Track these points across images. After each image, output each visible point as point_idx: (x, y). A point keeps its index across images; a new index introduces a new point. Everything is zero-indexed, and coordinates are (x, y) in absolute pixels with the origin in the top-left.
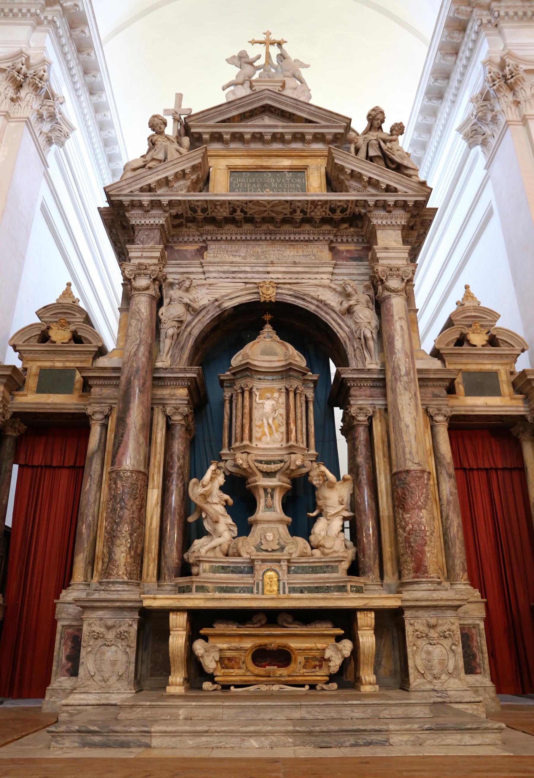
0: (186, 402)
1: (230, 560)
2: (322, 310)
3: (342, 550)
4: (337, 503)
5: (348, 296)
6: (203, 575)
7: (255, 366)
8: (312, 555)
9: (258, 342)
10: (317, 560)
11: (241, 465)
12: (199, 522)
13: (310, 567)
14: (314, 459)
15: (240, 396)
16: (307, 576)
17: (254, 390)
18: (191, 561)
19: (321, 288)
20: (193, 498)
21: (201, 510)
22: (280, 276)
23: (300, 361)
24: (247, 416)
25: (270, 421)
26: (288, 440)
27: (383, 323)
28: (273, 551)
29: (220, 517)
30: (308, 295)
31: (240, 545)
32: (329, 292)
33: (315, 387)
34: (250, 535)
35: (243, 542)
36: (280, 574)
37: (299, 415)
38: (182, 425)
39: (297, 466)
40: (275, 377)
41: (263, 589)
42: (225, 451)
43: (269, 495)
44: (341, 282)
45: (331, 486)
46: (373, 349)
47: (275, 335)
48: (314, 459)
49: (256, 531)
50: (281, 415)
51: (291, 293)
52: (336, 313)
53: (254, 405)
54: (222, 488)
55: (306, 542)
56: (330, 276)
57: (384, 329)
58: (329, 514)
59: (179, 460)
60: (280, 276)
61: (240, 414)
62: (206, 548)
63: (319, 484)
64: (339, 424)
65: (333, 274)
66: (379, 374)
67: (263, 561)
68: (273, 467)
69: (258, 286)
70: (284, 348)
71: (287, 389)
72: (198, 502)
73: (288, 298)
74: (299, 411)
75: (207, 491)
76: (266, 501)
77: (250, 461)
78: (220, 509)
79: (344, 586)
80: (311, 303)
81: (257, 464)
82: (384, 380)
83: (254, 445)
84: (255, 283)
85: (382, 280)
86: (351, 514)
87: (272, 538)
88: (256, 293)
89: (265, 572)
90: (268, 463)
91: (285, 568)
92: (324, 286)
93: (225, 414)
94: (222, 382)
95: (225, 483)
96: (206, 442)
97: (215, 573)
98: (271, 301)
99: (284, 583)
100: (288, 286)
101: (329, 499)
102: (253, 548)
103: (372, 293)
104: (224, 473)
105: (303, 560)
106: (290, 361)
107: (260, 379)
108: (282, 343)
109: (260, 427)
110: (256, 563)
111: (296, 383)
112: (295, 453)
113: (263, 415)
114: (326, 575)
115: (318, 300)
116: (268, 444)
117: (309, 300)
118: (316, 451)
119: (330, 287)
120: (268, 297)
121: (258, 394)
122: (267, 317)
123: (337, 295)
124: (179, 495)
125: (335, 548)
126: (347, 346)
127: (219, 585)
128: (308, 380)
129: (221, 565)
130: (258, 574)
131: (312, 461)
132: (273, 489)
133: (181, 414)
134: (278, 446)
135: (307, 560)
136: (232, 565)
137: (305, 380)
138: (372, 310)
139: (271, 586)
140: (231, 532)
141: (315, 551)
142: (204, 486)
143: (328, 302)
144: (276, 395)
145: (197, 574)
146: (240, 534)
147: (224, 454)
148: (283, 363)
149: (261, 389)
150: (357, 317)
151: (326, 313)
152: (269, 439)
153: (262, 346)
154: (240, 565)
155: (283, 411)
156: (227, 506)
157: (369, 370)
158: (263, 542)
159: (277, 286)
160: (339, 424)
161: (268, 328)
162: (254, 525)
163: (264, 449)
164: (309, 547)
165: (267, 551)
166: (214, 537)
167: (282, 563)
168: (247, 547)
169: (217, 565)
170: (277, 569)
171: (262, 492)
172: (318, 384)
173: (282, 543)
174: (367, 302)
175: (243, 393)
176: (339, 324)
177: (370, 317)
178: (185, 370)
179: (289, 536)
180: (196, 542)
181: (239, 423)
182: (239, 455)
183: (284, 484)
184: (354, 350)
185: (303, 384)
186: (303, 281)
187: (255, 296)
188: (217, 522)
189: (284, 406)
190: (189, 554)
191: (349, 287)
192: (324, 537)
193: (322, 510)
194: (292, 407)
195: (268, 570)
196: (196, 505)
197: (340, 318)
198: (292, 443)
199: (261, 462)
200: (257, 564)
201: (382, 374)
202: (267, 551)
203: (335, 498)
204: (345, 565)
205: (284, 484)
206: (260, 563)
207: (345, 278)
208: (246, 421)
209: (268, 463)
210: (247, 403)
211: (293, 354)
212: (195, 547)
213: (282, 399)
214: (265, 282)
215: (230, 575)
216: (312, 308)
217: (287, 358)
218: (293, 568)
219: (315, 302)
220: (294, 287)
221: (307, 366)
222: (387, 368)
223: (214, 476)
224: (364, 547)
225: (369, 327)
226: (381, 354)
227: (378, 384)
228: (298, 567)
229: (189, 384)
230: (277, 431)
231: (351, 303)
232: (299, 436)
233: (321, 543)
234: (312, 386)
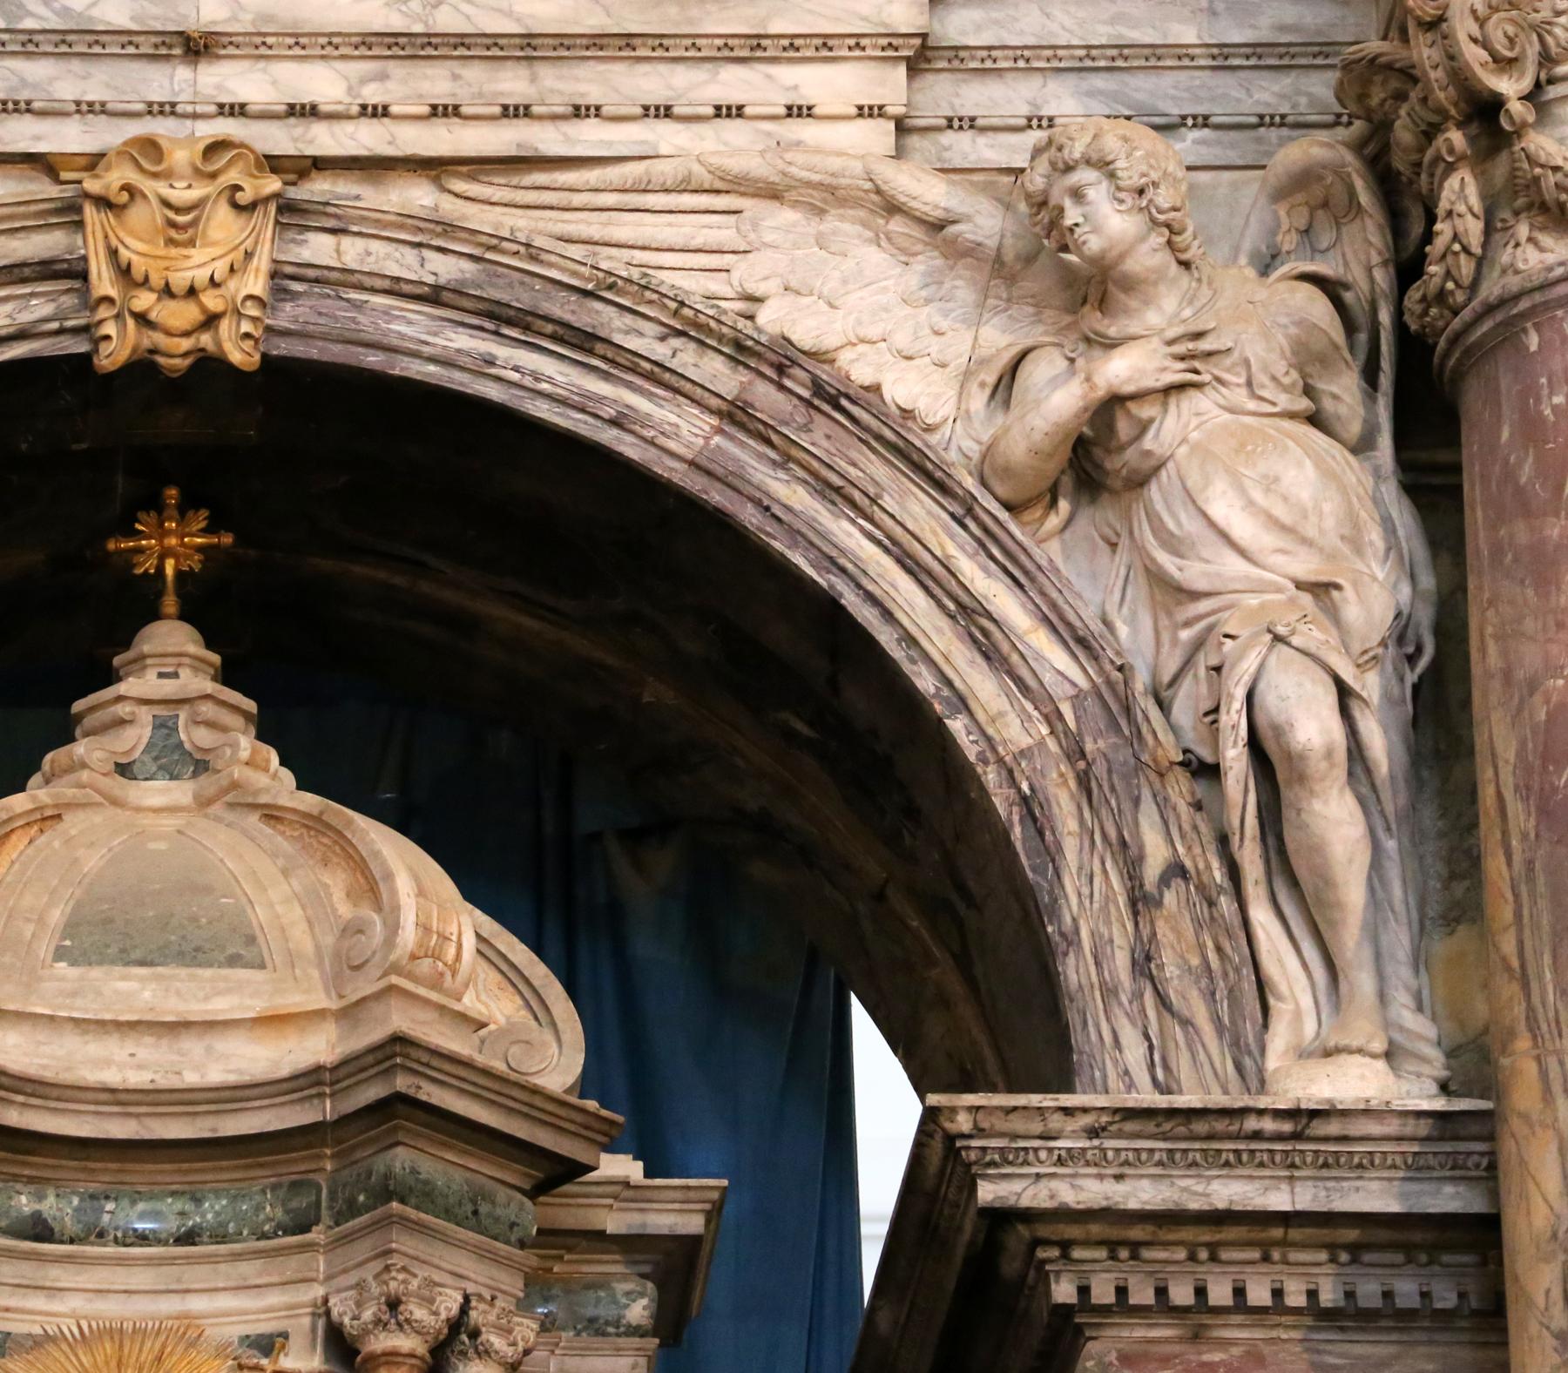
2: (786, 457)
5: (1087, 293)
9: (49, 818)
19: (779, 221)
22: (323, 83)
23: (507, 1014)
27: (1479, 587)
30: (630, 293)
32: (875, 258)
33: (672, 1325)
40: (210, 1212)
44: (1014, 150)
46: (1353, 892)
47: (247, 743)
51: (444, 268)
52: (938, 483)
56: (890, 88)
57: (1486, 657)
60: (323, 83)
65: (921, 56)
66: (1417, 1169)
69: (72, 194)
70: (336, 883)
73: (411, 323)
80: (659, 377)
82: (1482, 1235)
84: (43, 164)
85: (1484, 112)
88: (47, 270)
92: (824, 196)
98: (209, 366)
100: (418, 196)
103: (1360, 254)
106: (400, 1019)
107: (40, 1230)
108: (314, 823)
115: (741, 351)
117: (645, 342)
119: (893, 208)
120: (181, 314)
122: (171, 545)
123: (963, 290)
126: (1051, 854)
128: (599, 1239)
137: (553, 1239)
138: (1362, 446)
143: (860, 369)
148: (319, 1047)
150: (1185, 523)
151: (834, 492)
153: (92, 861)
157: (1298, 1114)
159: (292, 190)
161: (170, 666)
172: (714, 1291)
174: (1308, 362)
176: (968, 614)
177: (1327, 519)
184: (1140, 901)
185: (537, 1286)
186: (589, 137)
187: (41, 305)
191: (1099, 193)
197: (988, 541)
201: (1456, 1169)
207: (1063, 99)
211: (432, 944)
214: (151, 147)
216: (671, 435)
217: (366, 986)
219: (715, 372)
220: (487, 211)
221: (587, 1084)
222: (1524, 1095)
225: (1313, 636)
226: (1440, 947)
227: (1407, 1290)
231: (1122, 369)
234: (638, 1311)
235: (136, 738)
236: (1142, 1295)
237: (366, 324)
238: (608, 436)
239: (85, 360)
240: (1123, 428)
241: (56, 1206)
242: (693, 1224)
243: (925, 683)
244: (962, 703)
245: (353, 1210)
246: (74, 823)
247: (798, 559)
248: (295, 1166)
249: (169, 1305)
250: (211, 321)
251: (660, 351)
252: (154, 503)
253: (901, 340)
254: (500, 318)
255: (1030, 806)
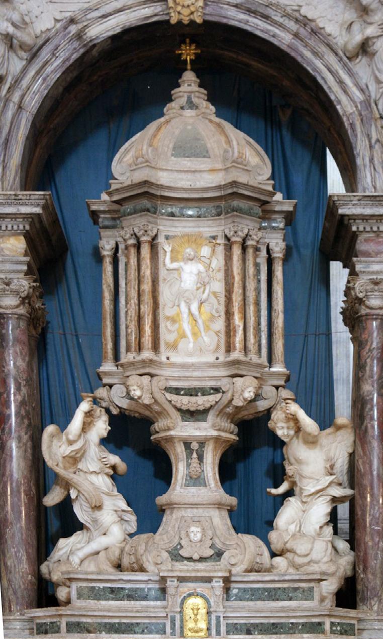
0: (25, 268)
1: (125, 578)
2: (306, 46)
3: (326, 559)
4: (323, 471)
6: (77, 603)
7: (161, 187)
8: (272, 567)
9: (168, 122)
10: (276, 578)
11: (139, 398)
12: (66, 505)
13: (265, 590)
14: (282, 383)
15: (133, 251)
16: (260, 604)
17: (161, 239)
18: (55, 577)
20: (50, 463)
21: (67, 485)
24: (147, 298)
25: (194, 307)
26: (229, 348)
28: (202, 559)
29: (104, 497)
31: (141, 549)
34: (161, 529)
35: (147, 543)
36: (212, 601)
37: (251, 295)
38: (20, 317)
39: (245, 400)
41: (182, 627)
42: (108, 367)
43: (195, 455)
45: (311, 441)
48: (282, 383)
49: (170, 521)
50: (215, 294)
53: (162, 273)
54: (104, 442)
55: (261, 543)
58: (306, 493)
59: (18, 389)
61: (134, 294)
62: (81, 554)
63: (288, 436)
64: (338, 301)
67: (182, 579)
68: (201, 402)
71: (227, 238)
72: (60, 470)
74: (251, 285)
75: (77, 451)
76: (189, 465)
77: (155, 390)
78: (104, 483)
79: (319, 624)
80: (281, 26)
81: (169, 396)
83: (164, 359)
86: (349, 492)
87: (199, 536)
89: (185, 598)
90: (191, 392)
91: (219, 591)
93: (104, 287)
94: (94, 215)
95: (109, 432)
96: (69, 337)
97: (99, 599)
98: (192, 22)
99: (218, 618)
101: (307, 464)
102: (165, 555)
104: (108, 411)
105: (253, 576)
107: (172, 215)
108: (219, 125)
109: (173, 320)
110: (169, 583)
111: (246, 226)
112: (242, 376)
113: (180, 294)
114: (293, 604)
115: (297, 21)
116: (190, 355)
117: (278, 18)
118: (287, 367)
121: (168, 249)
124: (25, 458)
125: (315, 556)
126: (356, 136)
127: (107, 621)
129: (109, 585)
130: (173, 601)
131: (277, 388)
132: (202, 443)
133: (16, 293)
134: (211, 359)
135: (259, 578)
136: (128, 586)
139: (196, 621)
140: (125, 525)
141: (277, 560)
142: (71, 443)
144: (206, 251)
145: (68, 602)
146: (140, 530)
147: (106, 374)
149: (174, 237)
151: (316, 54)
152: (191, 345)
154: (142, 586)
155: (219, 286)
156: (115, 476)
158: (183, 542)
160: (338, 301)
161: (189, 84)
162: (168, 512)
163: (184, 366)
164: (267, 554)
165: (190, 559)
166: (95, 533)
167: (214, 584)
168: (154, 552)
169: (102, 585)
170: (206, 593)
171: (180, 449)
173: (219, 545)
175: (138, 246)
176: (341, 83)
178: (17, 201)
179: (233, 531)
180: (62, 542)
181: (133, 313)
182: (134, 381)
183: (223, 434)
184: (371, 147)
188: (98, 507)
189: (221, 275)
190: (51, 565)
192: (294, 535)
193: (294, 484)
194: (237, 278)
195: (190, 595)
196: (56, 475)
197: (345, 65)
198: (236, 355)
199: (177, 391)
200: (171, 585)
202: (190, 559)
203: (317, 462)
204: (330, 586)
205: (223, 434)
206: (176, 583)
208: (146, 309)
209: (191, 392)
210: (147, 271)
212: (61, 552)
213: (218, 262)
215: (126, 602)
216: (283, 39)
218: (235, 591)
223: (89, 420)
224: (366, 554)
228: (245, 590)
229: (27, 227)
230: (207, 328)
232: (252, 339)
233: (288, 546)
235: (183, 101)
236: (368, 229)
237: (223, 12)
238: (271, 39)
239: (168, 22)
240: (370, 43)
241: (175, 210)
242: (291, 209)
243: (333, 97)
244: (339, 102)
245: (227, 213)
246: (173, 122)
247: (309, 69)
248: (217, 203)
249: (196, 230)
250: (192, 13)
251: (281, 20)
252: (184, 43)
253: (329, 17)
254: (249, 11)
255: (352, 125)
